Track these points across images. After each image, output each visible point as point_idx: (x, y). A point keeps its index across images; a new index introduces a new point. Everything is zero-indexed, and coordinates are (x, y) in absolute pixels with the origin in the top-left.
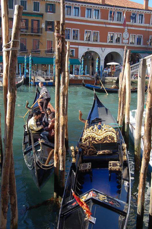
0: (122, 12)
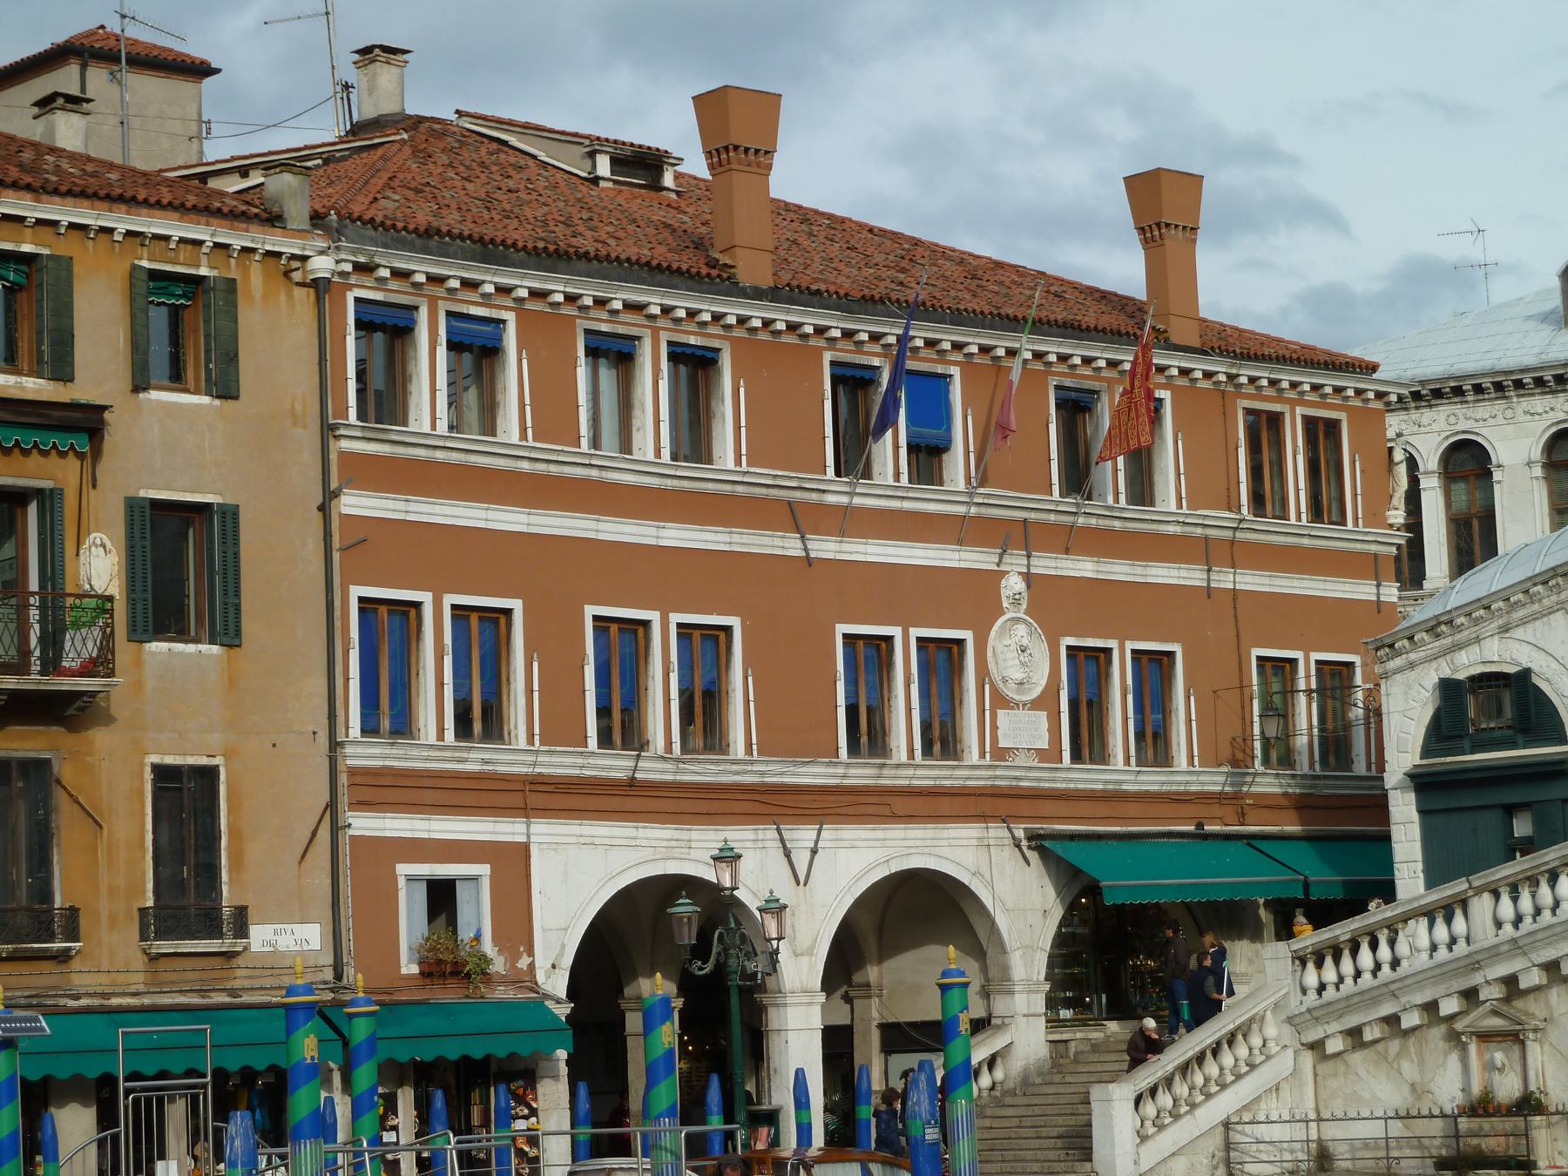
0: (955, 371)
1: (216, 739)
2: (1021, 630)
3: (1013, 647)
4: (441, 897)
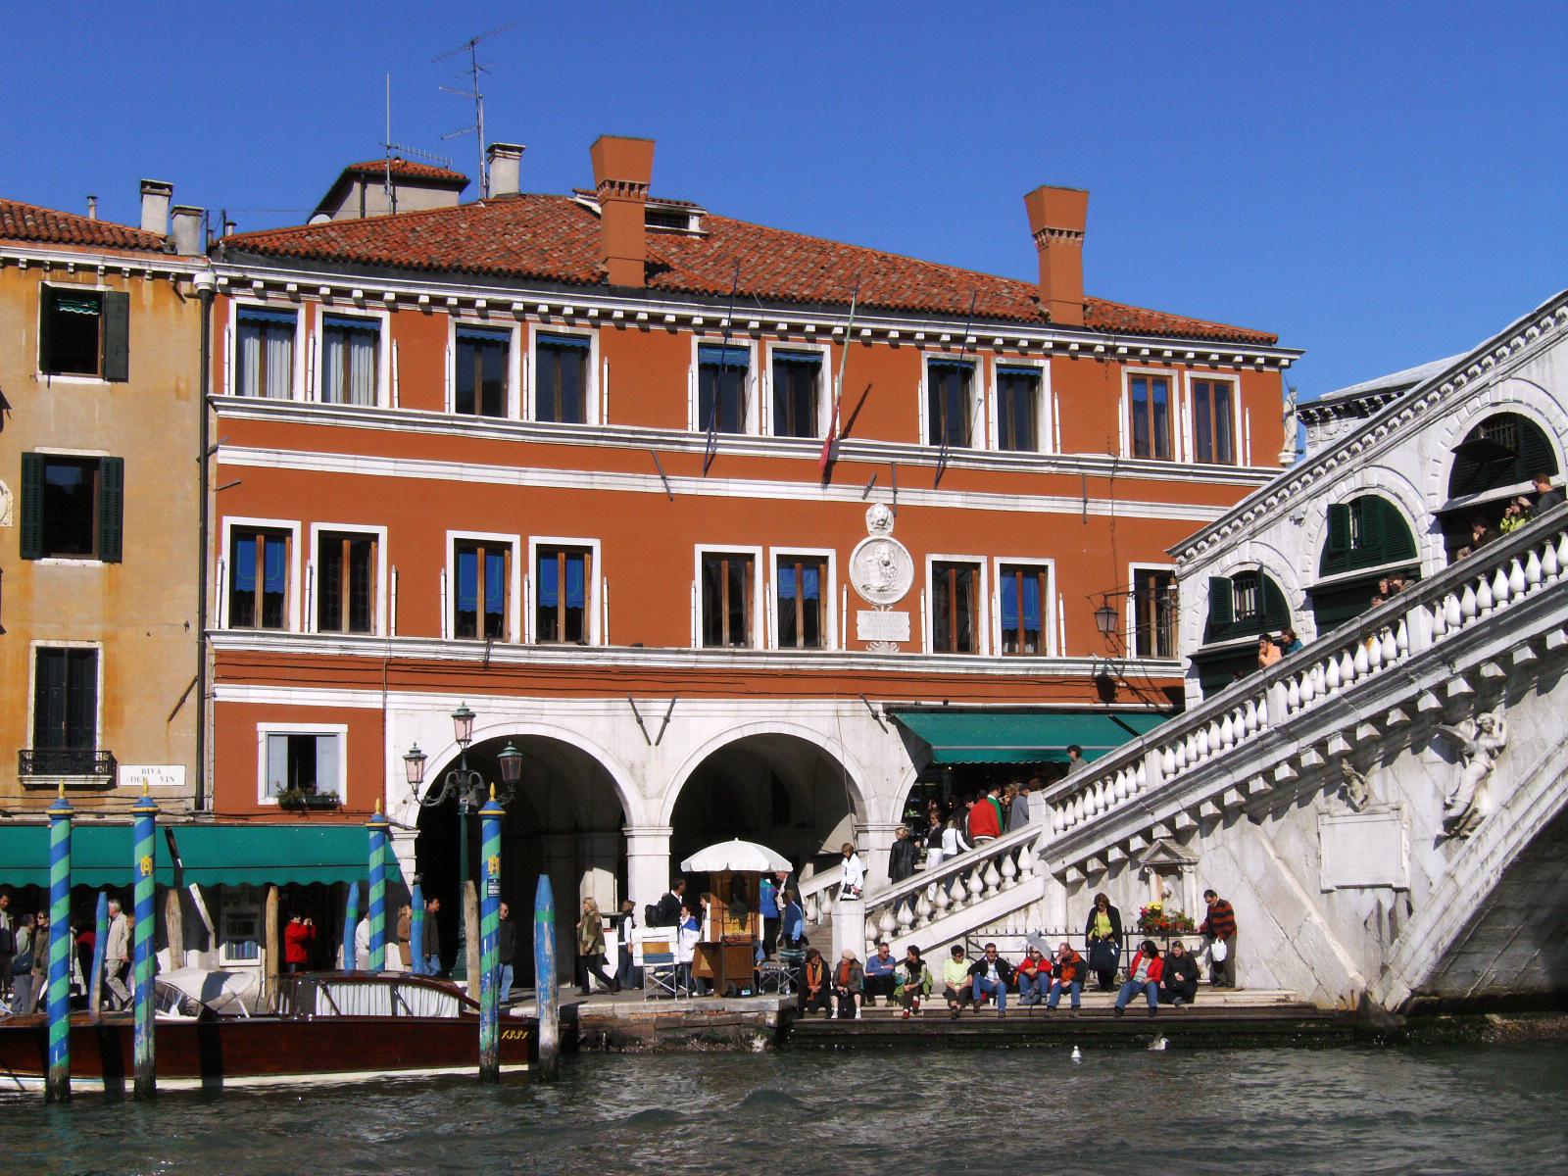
1: (96, 629)
2: (884, 548)
3: (875, 562)
4: (302, 752)
